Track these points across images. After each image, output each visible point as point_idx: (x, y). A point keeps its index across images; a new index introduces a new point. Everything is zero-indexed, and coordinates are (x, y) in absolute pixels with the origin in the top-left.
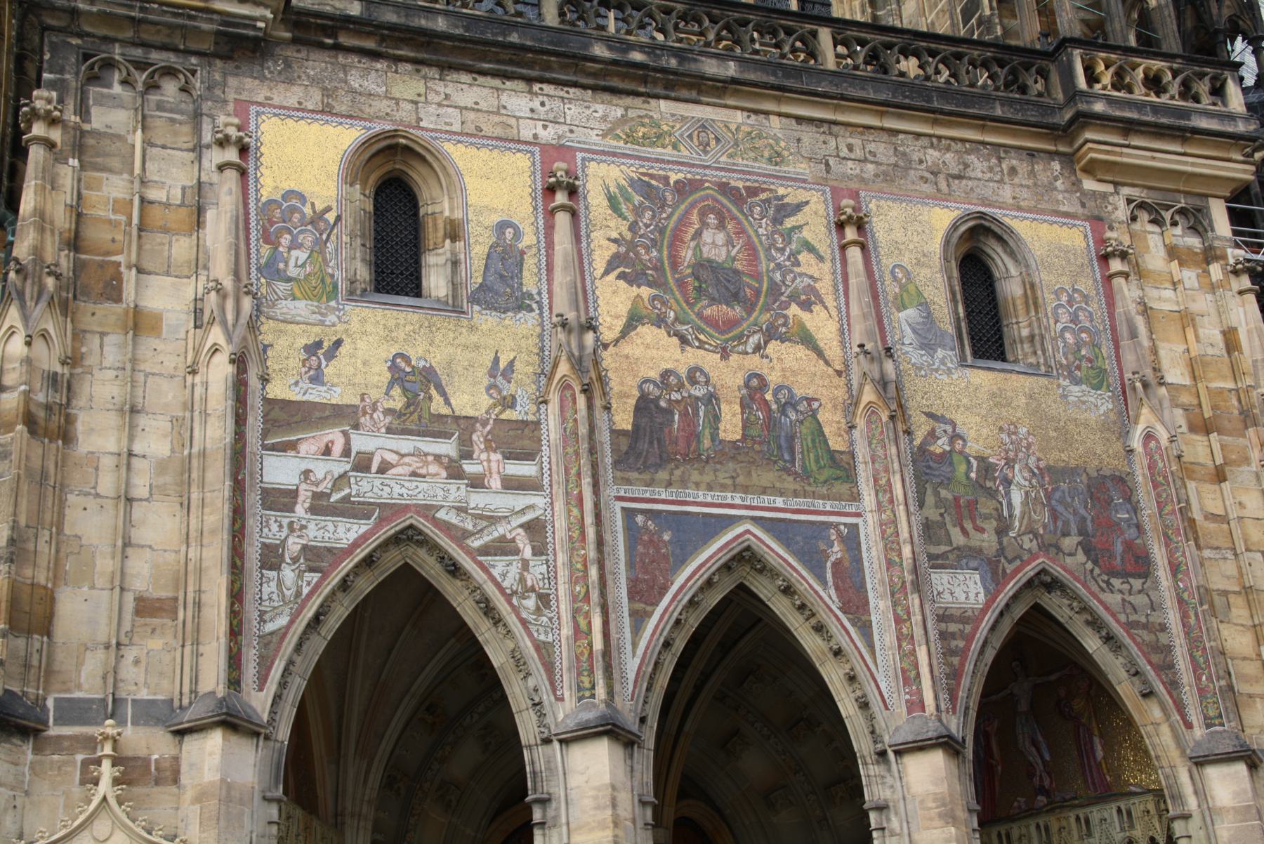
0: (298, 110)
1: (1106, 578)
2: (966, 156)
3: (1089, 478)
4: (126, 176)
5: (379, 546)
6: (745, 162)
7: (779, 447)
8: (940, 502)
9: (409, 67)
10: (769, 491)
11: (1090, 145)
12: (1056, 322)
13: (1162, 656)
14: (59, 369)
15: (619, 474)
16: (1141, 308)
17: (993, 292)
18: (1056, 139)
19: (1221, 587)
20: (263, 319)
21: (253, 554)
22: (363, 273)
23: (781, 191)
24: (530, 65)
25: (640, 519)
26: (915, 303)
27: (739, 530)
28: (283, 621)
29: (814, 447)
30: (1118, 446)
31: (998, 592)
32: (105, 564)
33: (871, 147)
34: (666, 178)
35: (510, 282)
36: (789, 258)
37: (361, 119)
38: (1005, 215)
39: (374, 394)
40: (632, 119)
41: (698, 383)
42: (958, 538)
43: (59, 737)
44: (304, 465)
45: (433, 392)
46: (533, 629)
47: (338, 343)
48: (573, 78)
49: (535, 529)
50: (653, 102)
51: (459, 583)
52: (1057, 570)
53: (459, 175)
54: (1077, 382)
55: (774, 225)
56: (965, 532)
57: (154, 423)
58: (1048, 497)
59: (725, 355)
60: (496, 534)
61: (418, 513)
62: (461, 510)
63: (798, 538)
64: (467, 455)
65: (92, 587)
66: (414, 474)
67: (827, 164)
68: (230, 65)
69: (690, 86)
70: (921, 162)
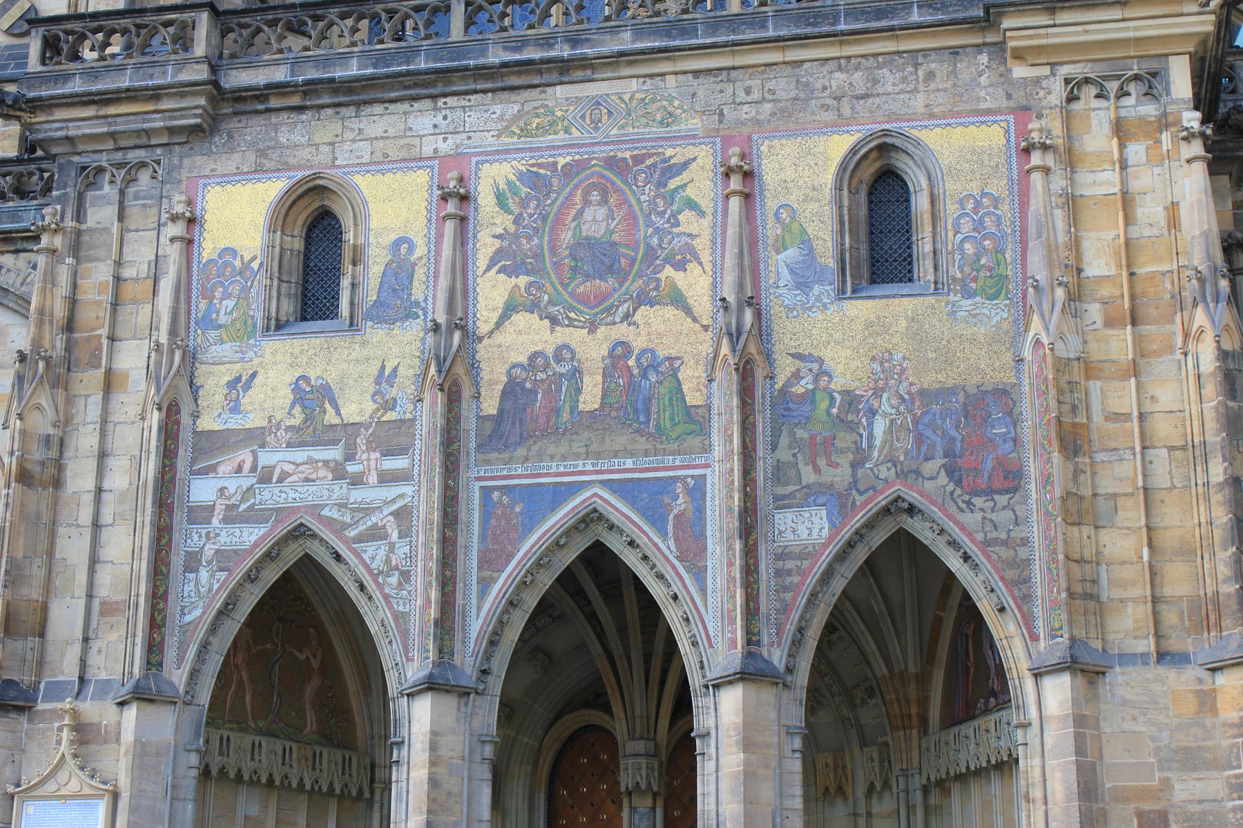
0: (236, 174)
1: (967, 497)
2: (876, 71)
3: (967, 396)
4: (109, 262)
5: (277, 543)
6: (636, 130)
7: (636, 411)
8: (794, 442)
9: (329, 111)
10: (620, 454)
11: (1008, 34)
12: (956, 233)
13: (1018, 572)
14: (51, 431)
15: (481, 456)
16: (1062, 200)
17: (908, 208)
18: (983, 29)
19: (1110, 491)
20: (197, 365)
21: (177, 561)
22: (288, 308)
23: (669, 152)
24: (432, 84)
25: (496, 495)
26: (798, 242)
27: (588, 494)
28: (197, 613)
29: (671, 405)
30: (1008, 358)
31: (845, 525)
32: (82, 578)
33: (771, 85)
34: (555, 164)
35: (401, 294)
36: (669, 220)
37: (288, 170)
38: (913, 127)
39: (279, 415)
40: (528, 113)
41: (564, 360)
42: (808, 476)
43: (44, 710)
44: (221, 484)
45: (327, 405)
46: (394, 601)
47: (254, 375)
48: (472, 87)
49: (403, 515)
50: (549, 90)
51: (343, 567)
52: (912, 496)
53: (365, 203)
54: (969, 295)
55: (658, 189)
56: (817, 469)
57: (119, 463)
58: (916, 422)
59: (592, 327)
60: (369, 523)
61: (306, 512)
62: (342, 506)
63: (645, 495)
64: (350, 457)
65: (73, 597)
66: (307, 480)
67: (721, 114)
68: (187, 147)
69: (584, 67)
70: (824, 88)
